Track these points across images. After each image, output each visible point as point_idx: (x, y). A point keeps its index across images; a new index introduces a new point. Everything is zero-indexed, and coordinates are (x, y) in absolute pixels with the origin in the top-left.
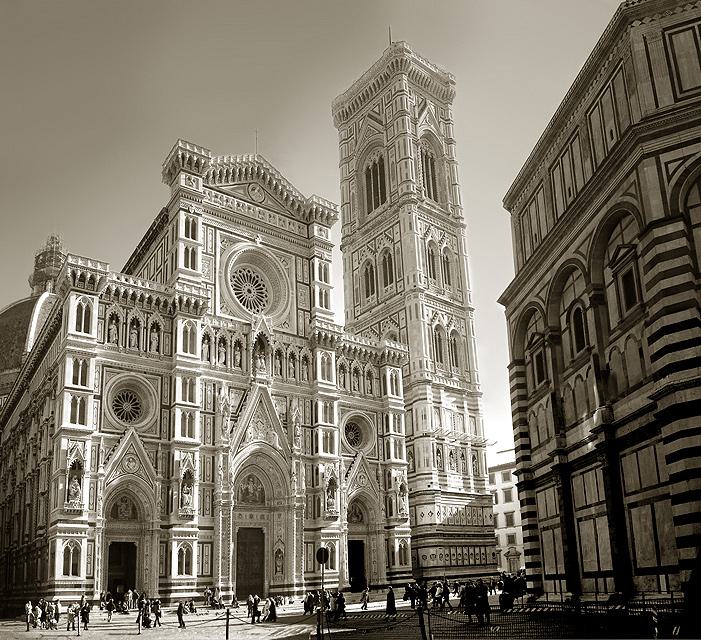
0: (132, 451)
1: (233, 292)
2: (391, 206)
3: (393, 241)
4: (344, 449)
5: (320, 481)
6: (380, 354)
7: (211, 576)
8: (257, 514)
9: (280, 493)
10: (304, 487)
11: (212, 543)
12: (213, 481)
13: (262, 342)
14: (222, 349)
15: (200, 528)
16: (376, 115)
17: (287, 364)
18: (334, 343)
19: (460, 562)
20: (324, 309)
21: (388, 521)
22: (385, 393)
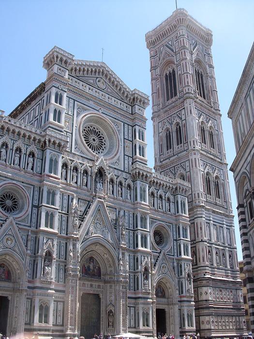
0: (10, 233)
1: (85, 142)
3: (181, 119)
4: (153, 247)
5: (139, 267)
6: (174, 187)
7: (63, 325)
8: (95, 284)
9: (111, 271)
10: (128, 269)
11: (63, 302)
12: (66, 259)
13: (101, 173)
14: (75, 174)
15: (55, 290)
16: (170, 46)
17: (117, 188)
18: (148, 179)
21: (181, 297)
22: (178, 212)
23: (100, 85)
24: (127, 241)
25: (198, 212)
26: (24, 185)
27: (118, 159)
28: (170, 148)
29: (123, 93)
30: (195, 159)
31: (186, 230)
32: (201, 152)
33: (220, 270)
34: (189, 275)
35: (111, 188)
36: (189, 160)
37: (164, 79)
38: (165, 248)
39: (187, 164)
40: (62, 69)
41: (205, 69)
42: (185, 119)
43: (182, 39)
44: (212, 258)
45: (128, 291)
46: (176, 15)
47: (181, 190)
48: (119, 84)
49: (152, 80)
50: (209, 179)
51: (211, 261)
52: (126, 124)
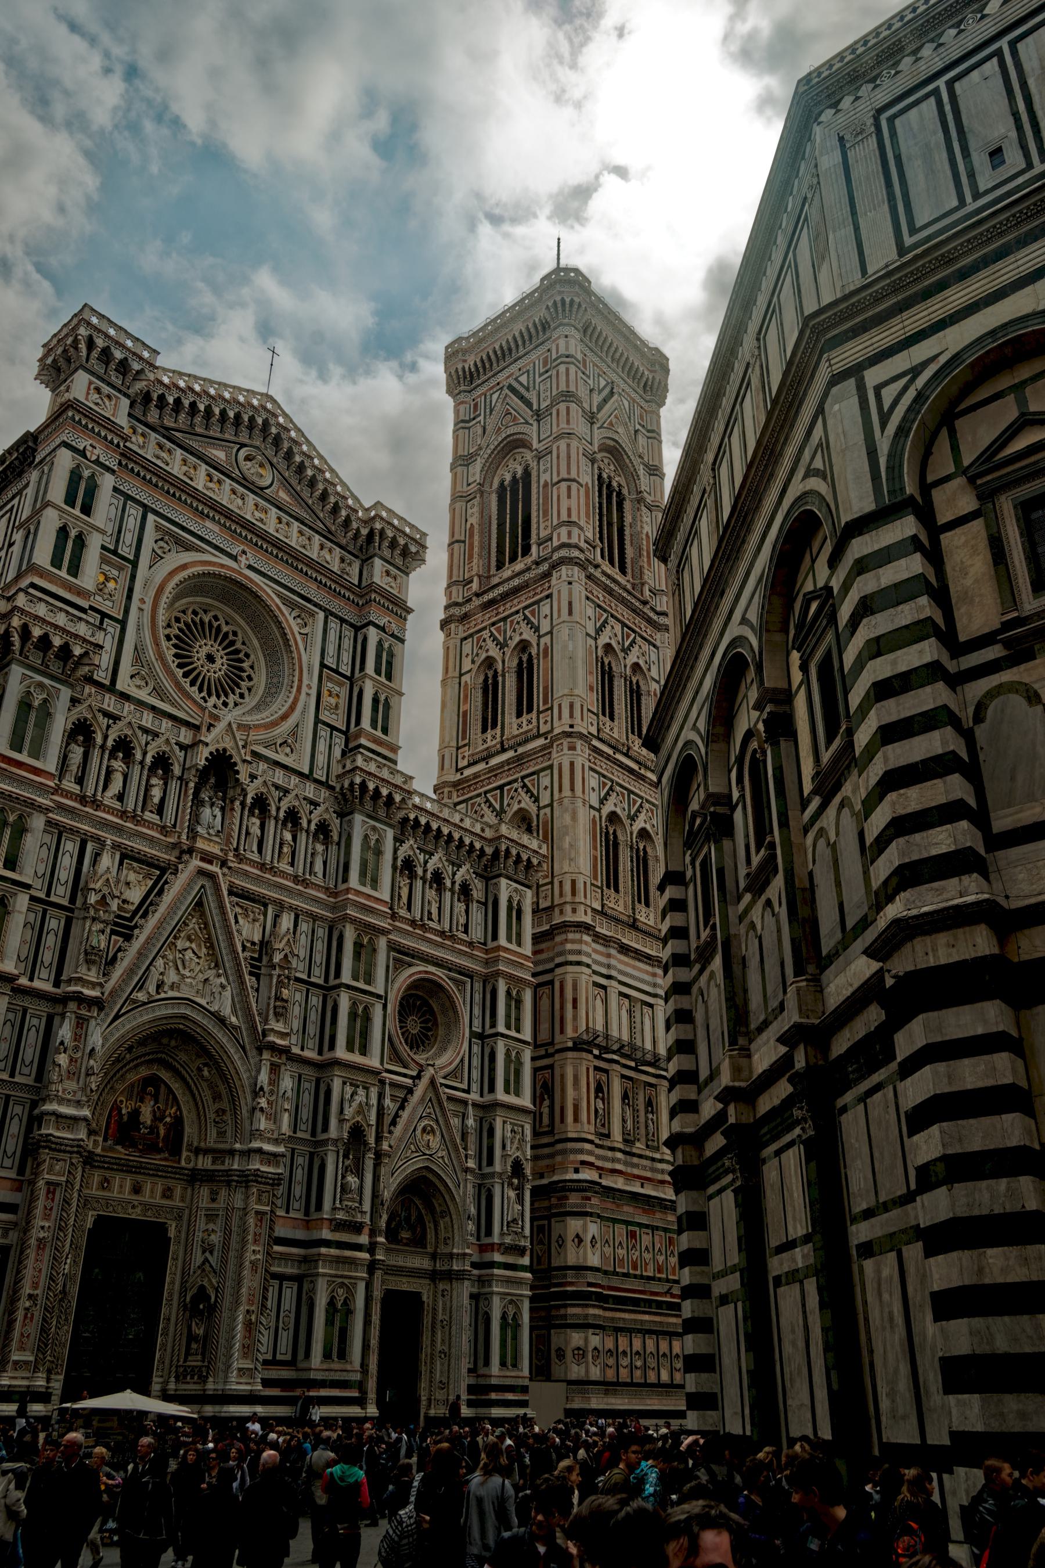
2: (537, 563)
3: (537, 629)
6: (489, 850)
12: (39, 1078)
14: (118, 765)
19: (638, 1373)
20: (379, 733)
21: (483, 1248)
22: (495, 937)
23: (250, 469)
24: (296, 1024)
25: (569, 946)
27: (294, 733)
28: (494, 726)
29: (336, 509)
30: (572, 764)
31: (519, 1002)
32: (595, 743)
33: (635, 1160)
34: (517, 1167)
35: (256, 830)
36: (551, 767)
37: (494, 499)
38: (439, 1062)
39: (545, 781)
40: (106, 389)
41: (633, 477)
42: (551, 633)
44: (608, 1112)
45: (281, 1213)
46: (552, 285)
47: (510, 861)
48: (319, 478)
49: (456, 497)
51: (603, 1119)
52: (336, 616)
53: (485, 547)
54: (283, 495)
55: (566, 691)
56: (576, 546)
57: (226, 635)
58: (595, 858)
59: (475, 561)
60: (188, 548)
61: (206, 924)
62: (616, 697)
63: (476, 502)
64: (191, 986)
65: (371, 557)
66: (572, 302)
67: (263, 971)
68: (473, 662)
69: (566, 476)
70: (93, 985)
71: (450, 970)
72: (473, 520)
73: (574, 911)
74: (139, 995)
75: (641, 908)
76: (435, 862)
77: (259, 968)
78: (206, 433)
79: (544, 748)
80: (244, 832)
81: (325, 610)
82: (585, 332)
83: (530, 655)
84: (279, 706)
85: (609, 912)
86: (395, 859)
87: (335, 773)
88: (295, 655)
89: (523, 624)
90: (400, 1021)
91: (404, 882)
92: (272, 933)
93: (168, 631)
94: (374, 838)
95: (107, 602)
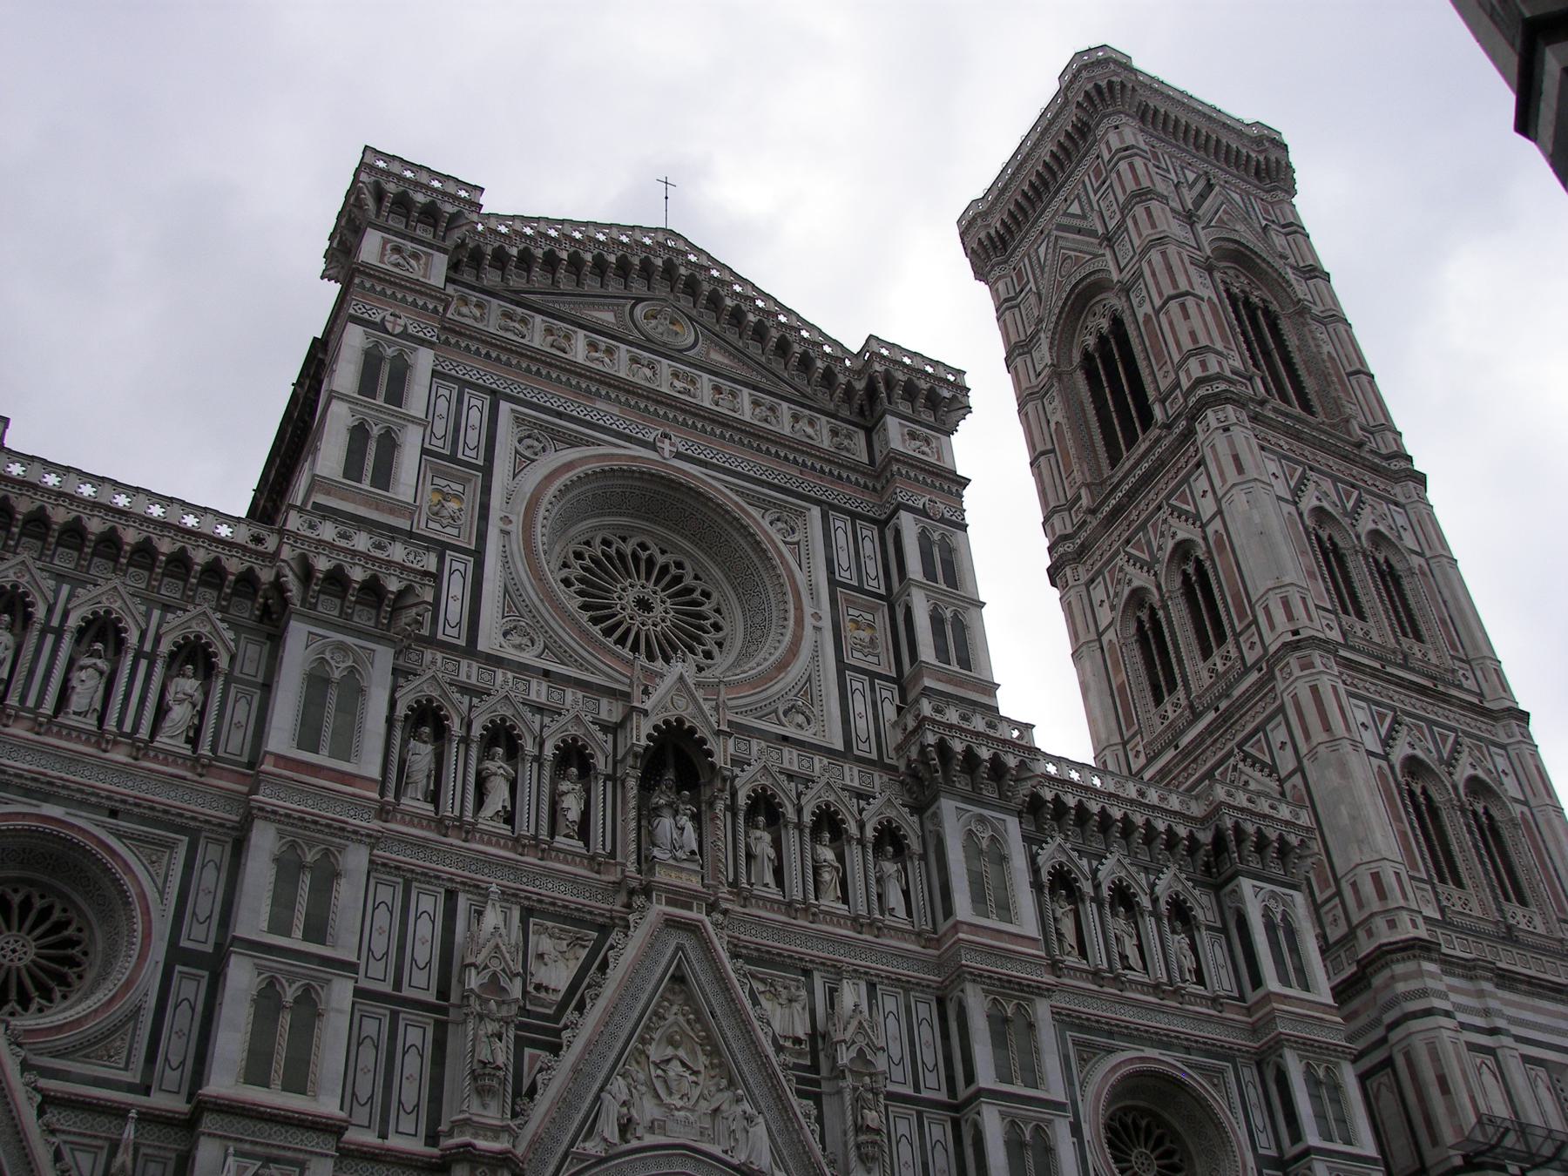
3: (1195, 518)
6: (1205, 837)
14: (497, 765)
16: (1077, 223)
22: (1257, 981)
26: (124, 824)
28: (1172, 687)
30: (1314, 690)
31: (1336, 1088)
36: (1281, 709)
41: (1279, 285)
42: (1220, 512)
43: (1123, 166)
46: (1075, 76)
47: (1249, 846)
50: (1428, 798)
53: (1087, 447)
54: (717, 357)
55: (1270, 584)
56: (1219, 377)
57: (664, 569)
58: (1403, 835)
59: (1076, 468)
60: (574, 442)
61: (697, 1012)
62: (1357, 585)
63: (1054, 391)
64: (687, 1123)
65: (882, 416)
66: (1110, 84)
67: (825, 1087)
68: (1113, 608)
69: (1172, 292)
70: (496, 1132)
71: (1188, 1050)
72: (1058, 416)
73: (1392, 924)
74: (588, 1145)
75: (1512, 908)
76: (1109, 870)
77: (817, 1083)
78: (578, 290)
79: (1260, 684)
80: (742, 853)
81: (818, 502)
82: (1143, 119)
83: (1199, 563)
84: (769, 654)
85: (1457, 919)
86: (1035, 870)
87: (892, 746)
88: (781, 570)
89: (1173, 521)
90: (1117, 1160)
91: (1063, 909)
92: (830, 1016)
93: (565, 573)
94: (985, 835)
95: (448, 530)
